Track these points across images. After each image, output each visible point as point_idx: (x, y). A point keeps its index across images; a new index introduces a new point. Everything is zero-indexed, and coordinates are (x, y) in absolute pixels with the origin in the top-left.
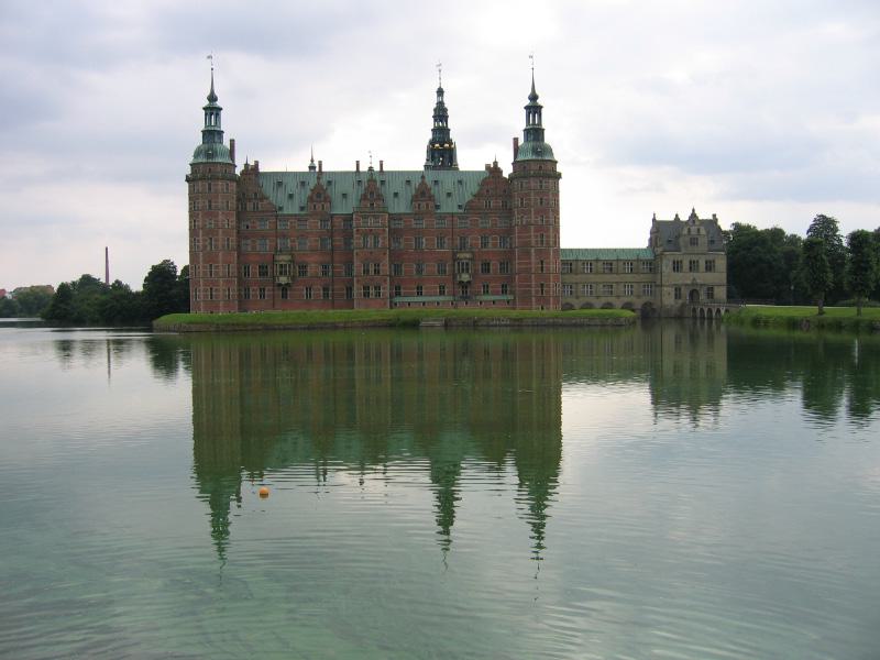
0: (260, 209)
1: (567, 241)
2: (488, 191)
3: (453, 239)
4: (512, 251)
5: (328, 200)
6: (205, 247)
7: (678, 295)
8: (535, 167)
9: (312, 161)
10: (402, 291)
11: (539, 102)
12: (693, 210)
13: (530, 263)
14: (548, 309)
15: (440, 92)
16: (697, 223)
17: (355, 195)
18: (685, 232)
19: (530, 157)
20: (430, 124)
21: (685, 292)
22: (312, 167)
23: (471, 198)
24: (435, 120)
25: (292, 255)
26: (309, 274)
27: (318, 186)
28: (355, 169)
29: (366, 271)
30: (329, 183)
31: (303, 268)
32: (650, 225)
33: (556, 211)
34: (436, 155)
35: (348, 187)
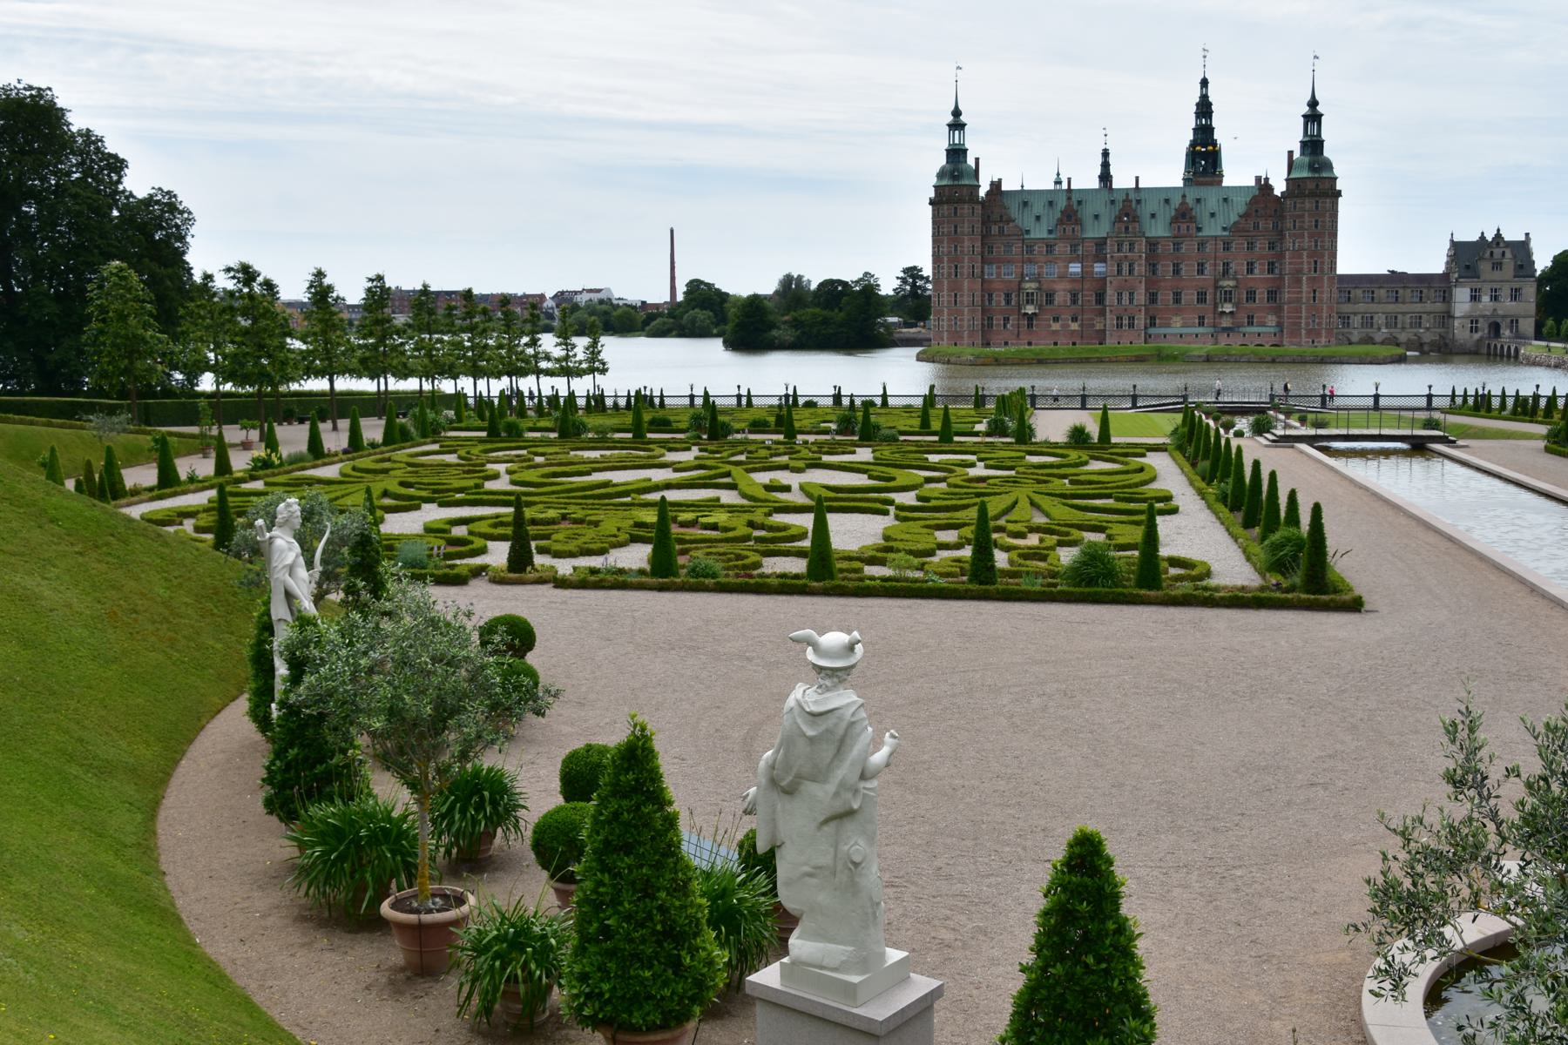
0: (1006, 233)
2: (1257, 211)
3: (1215, 265)
4: (1281, 278)
5: (1079, 222)
6: (949, 274)
7: (1474, 330)
8: (1310, 186)
9: (1058, 174)
10: (1157, 321)
12: (1498, 230)
13: (1301, 292)
14: (1319, 342)
16: (1501, 245)
18: (1487, 255)
19: (1305, 174)
20: (1191, 122)
22: (1058, 182)
23: (1237, 218)
24: (1197, 117)
25: (1040, 282)
26: (1056, 303)
27: (1069, 206)
29: (1119, 301)
30: (1080, 203)
31: (1050, 297)
32: (1448, 245)
33: (1334, 235)
34: (1197, 160)
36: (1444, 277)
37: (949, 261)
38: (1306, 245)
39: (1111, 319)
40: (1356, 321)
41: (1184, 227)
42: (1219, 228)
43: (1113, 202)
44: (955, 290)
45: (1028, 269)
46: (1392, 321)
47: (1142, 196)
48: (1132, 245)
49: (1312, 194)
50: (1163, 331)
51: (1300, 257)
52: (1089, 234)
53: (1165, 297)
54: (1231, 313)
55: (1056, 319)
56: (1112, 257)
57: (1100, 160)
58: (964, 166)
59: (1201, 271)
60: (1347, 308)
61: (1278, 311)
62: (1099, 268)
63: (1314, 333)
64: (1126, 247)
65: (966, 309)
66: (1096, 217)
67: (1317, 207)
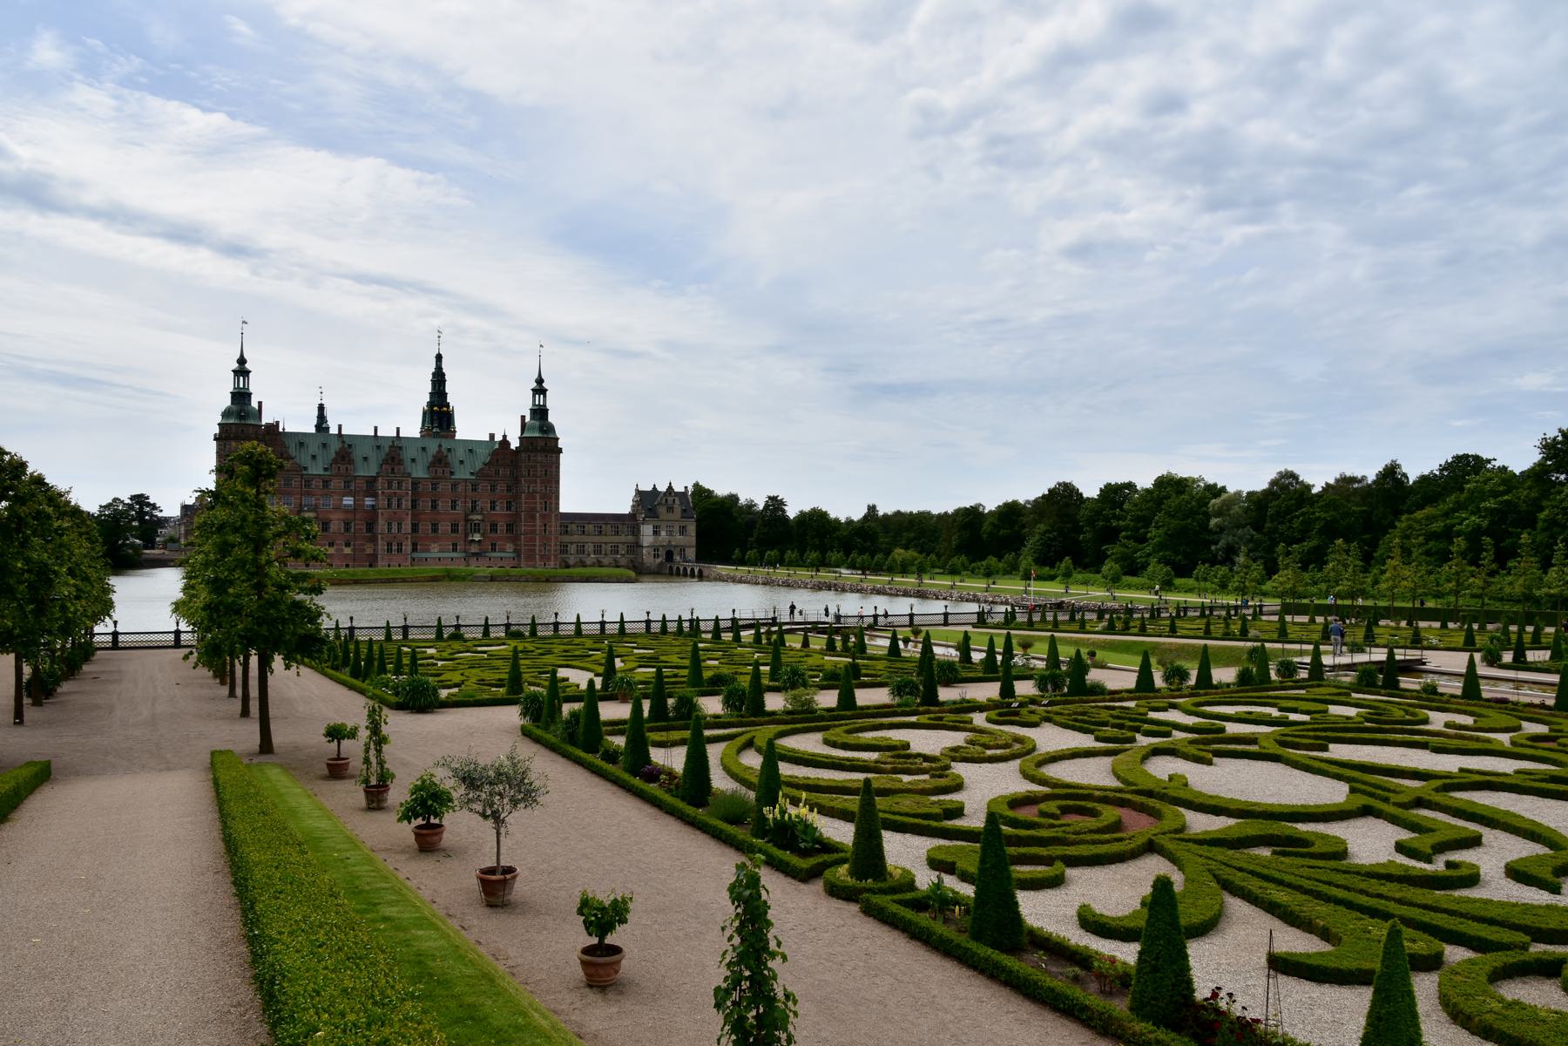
4: (518, 514)
5: (351, 462)
8: (541, 443)
11: (545, 385)
13: (535, 526)
15: (439, 358)
19: (537, 435)
20: (428, 387)
21: (662, 552)
25: (316, 512)
29: (390, 530)
35: (367, 451)
36: (631, 517)
38: (539, 490)
39: (381, 546)
40: (573, 548)
43: (378, 447)
46: (598, 549)
47: (403, 444)
49: (543, 450)
50: (424, 555)
51: (534, 498)
52: (361, 474)
53: (425, 527)
54: (479, 541)
56: (383, 493)
57: (316, 413)
59: (454, 507)
61: (515, 540)
62: (369, 501)
64: (395, 485)
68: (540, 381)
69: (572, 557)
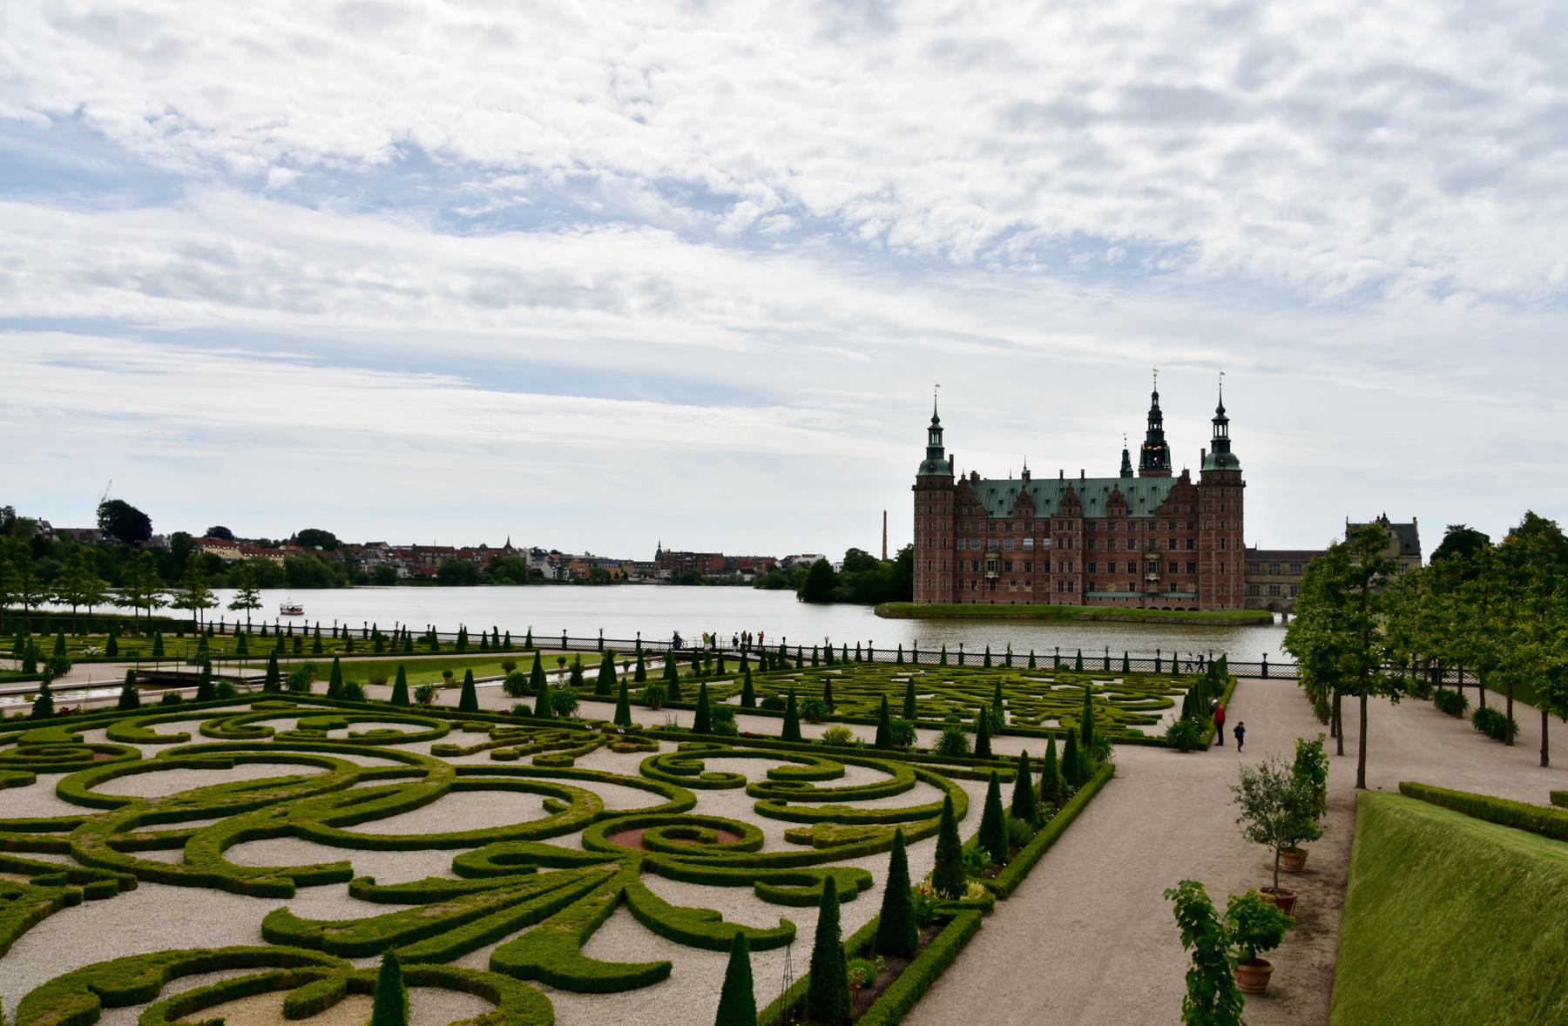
1: (1249, 542)
2: (1176, 498)
3: (1143, 541)
4: (1197, 554)
6: (925, 545)
8: (1217, 477)
12: (1384, 515)
13: (1210, 565)
15: (1155, 396)
17: (1056, 499)
19: (1212, 467)
20: (1145, 426)
25: (1000, 553)
27: (1023, 493)
28: (1059, 477)
30: (1035, 490)
31: (1009, 565)
32: (1344, 528)
37: (925, 535)
38: (1214, 526)
39: (1052, 586)
40: (1265, 590)
41: (1116, 510)
42: (1146, 512)
43: (1062, 490)
44: (929, 558)
45: (990, 542)
47: (1086, 485)
48: (1070, 524)
49: (1218, 484)
51: (1210, 535)
52: (1040, 515)
55: (1013, 583)
57: (1121, 459)
58: (939, 461)
59: (1131, 546)
60: (1255, 579)
61: (1195, 580)
62: (1047, 542)
63: (1223, 600)
64: (1066, 525)
65: (938, 574)
66: (1048, 501)
67: (1222, 494)
68: (1221, 410)
69: (1264, 599)
